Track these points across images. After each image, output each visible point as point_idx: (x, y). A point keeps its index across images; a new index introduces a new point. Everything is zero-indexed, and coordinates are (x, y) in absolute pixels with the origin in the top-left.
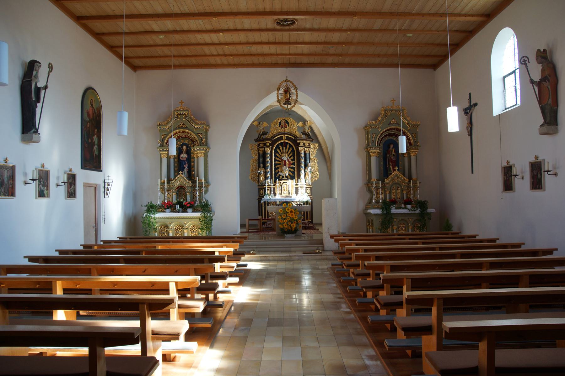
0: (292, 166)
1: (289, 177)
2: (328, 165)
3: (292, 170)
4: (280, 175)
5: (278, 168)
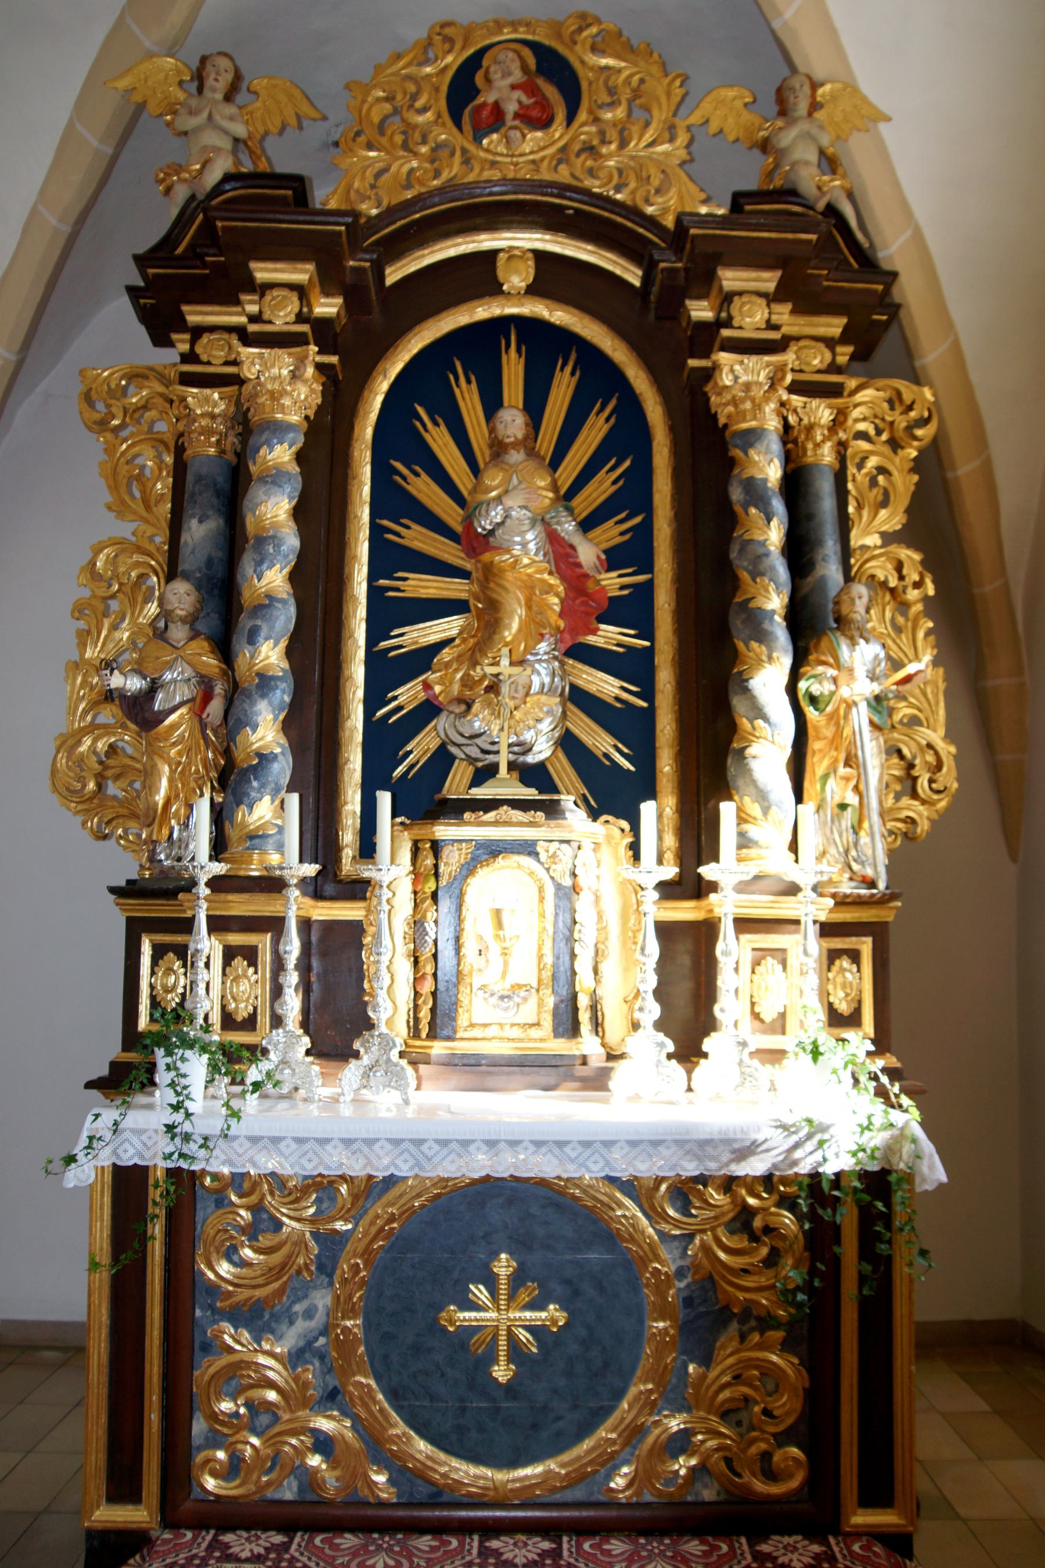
0: (608, 636)
1: (564, 772)
2: (1000, 680)
3: (607, 686)
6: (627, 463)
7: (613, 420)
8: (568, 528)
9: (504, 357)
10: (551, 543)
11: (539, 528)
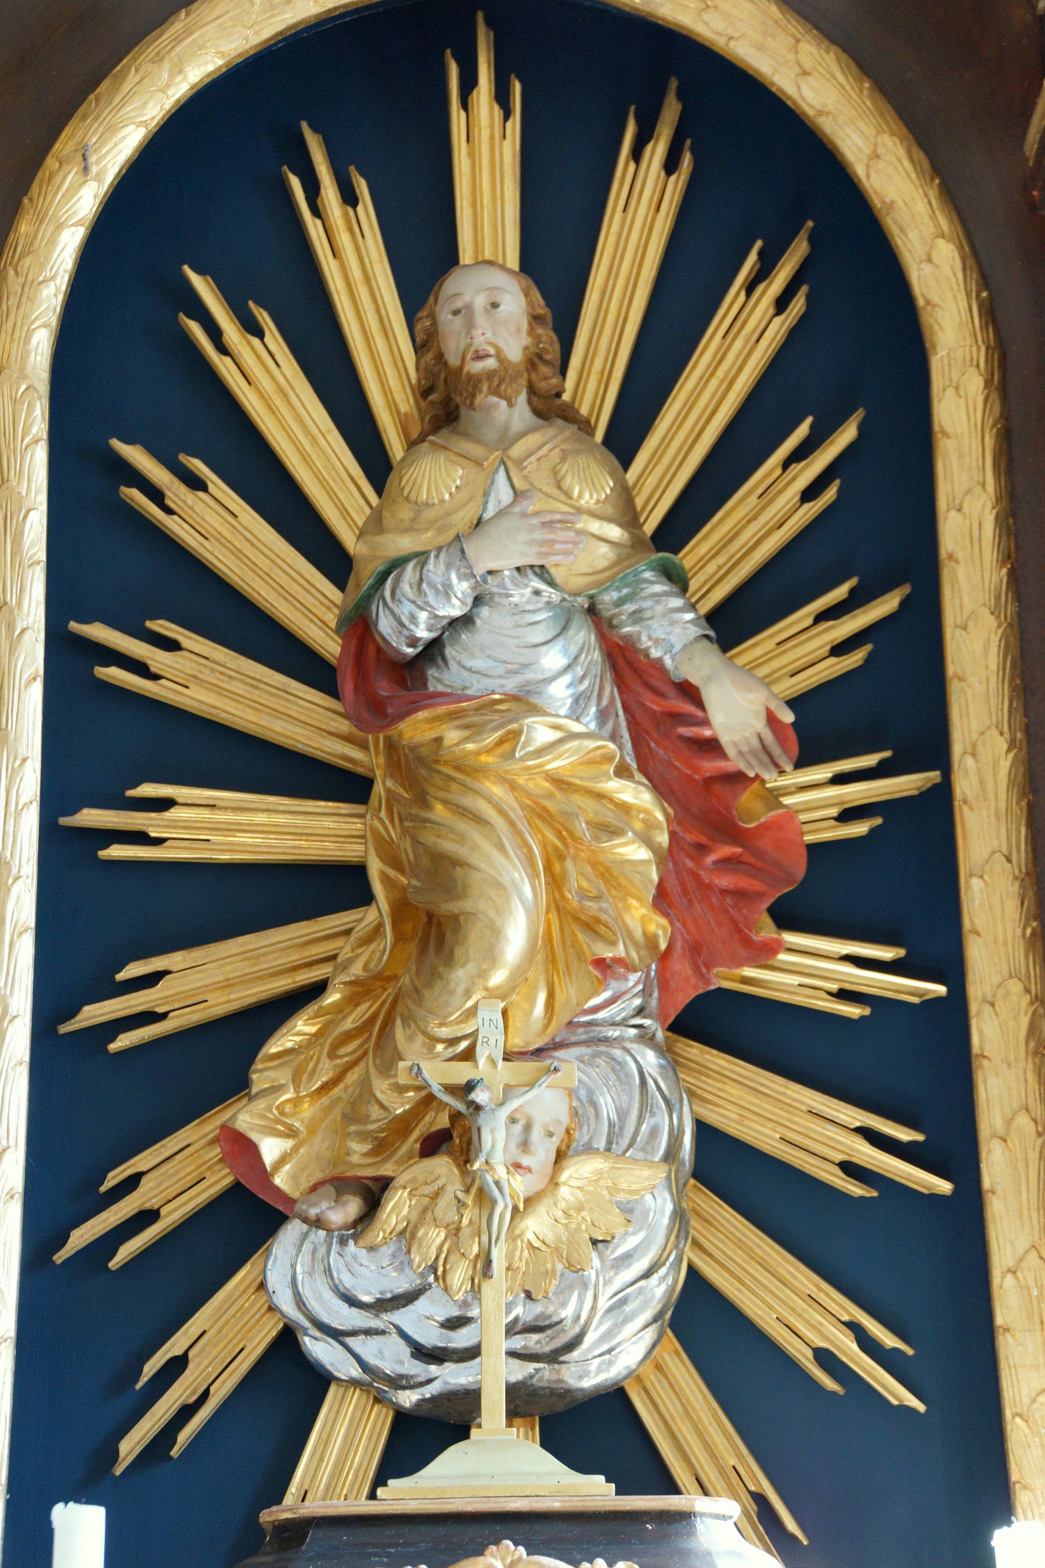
0: (812, 970)
1: (685, 1416)
4: (288, 1382)
5: (222, 1056)
6: (847, 435)
7: (798, 305)
8: (669, 630)
9: (458, 118)
10: (620, 681)
11: (582, 635)
